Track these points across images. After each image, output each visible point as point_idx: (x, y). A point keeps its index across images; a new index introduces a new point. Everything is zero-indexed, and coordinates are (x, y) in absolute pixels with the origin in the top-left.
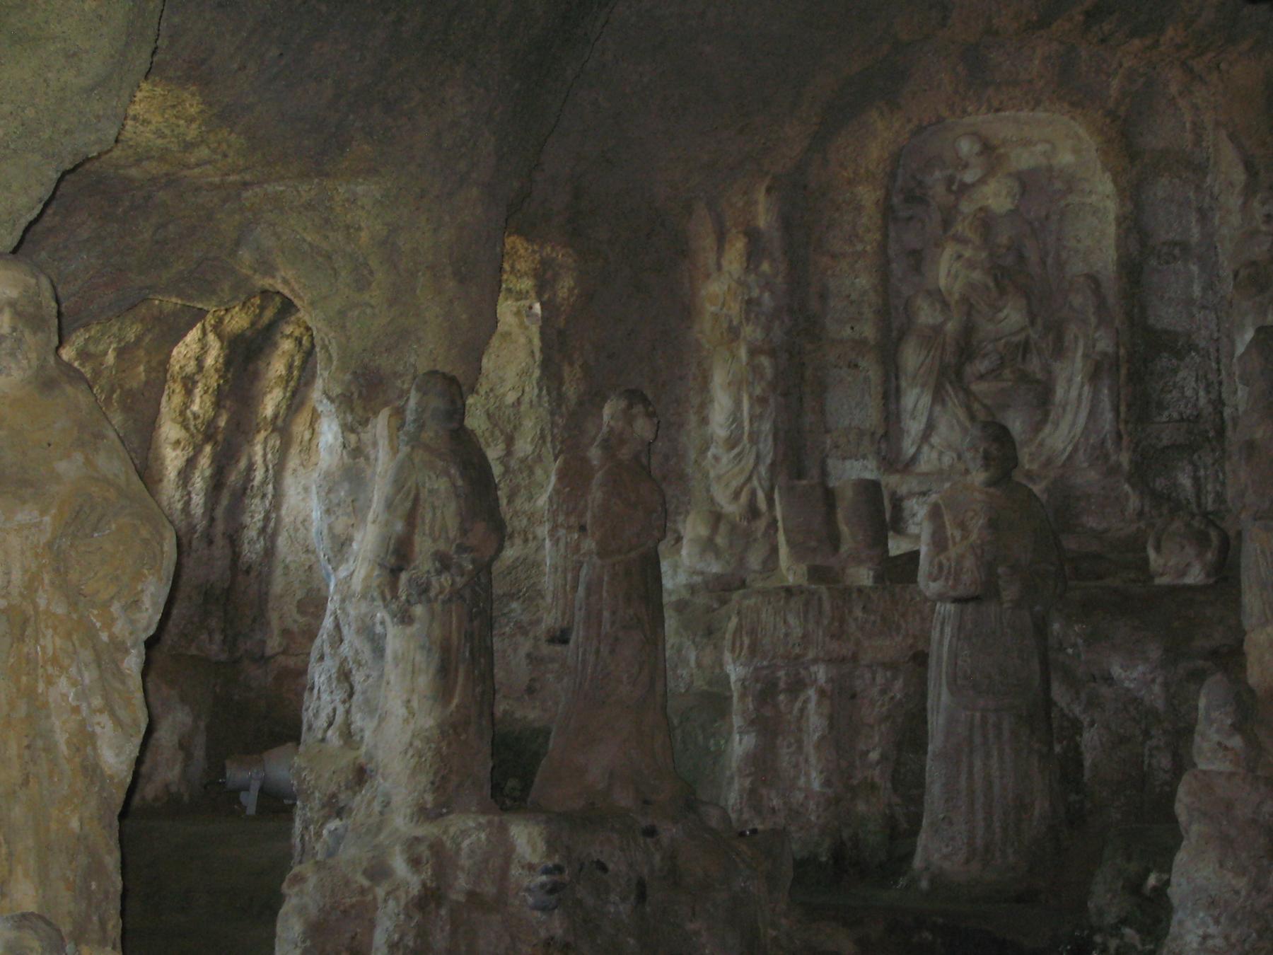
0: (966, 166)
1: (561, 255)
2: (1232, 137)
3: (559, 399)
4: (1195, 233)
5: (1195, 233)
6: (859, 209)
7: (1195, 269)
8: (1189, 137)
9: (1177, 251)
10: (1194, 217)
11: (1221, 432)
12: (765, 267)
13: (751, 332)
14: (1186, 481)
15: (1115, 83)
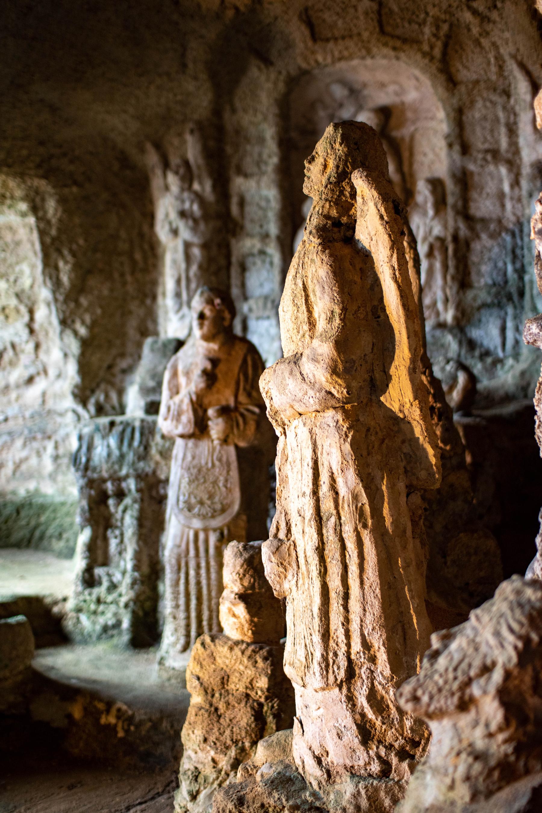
0: (341, 105)
1: (42, 184)
2: (522, 66)
3: (57, 284)
4: (504, 143)
5: (504, 143)
6: (261, 140)
7: (503, 170)
8: (494, 69)
9: (489, 157)
10: (503, 130)
11: (521, 294)
12: (196, 186)
13: (185, 234)
14: (494, 331)
15: (427, 31)
